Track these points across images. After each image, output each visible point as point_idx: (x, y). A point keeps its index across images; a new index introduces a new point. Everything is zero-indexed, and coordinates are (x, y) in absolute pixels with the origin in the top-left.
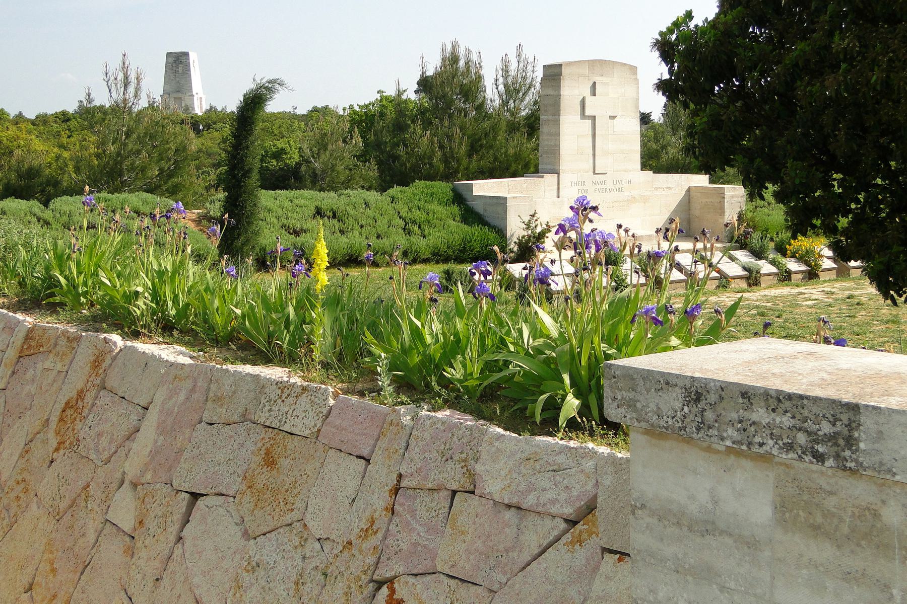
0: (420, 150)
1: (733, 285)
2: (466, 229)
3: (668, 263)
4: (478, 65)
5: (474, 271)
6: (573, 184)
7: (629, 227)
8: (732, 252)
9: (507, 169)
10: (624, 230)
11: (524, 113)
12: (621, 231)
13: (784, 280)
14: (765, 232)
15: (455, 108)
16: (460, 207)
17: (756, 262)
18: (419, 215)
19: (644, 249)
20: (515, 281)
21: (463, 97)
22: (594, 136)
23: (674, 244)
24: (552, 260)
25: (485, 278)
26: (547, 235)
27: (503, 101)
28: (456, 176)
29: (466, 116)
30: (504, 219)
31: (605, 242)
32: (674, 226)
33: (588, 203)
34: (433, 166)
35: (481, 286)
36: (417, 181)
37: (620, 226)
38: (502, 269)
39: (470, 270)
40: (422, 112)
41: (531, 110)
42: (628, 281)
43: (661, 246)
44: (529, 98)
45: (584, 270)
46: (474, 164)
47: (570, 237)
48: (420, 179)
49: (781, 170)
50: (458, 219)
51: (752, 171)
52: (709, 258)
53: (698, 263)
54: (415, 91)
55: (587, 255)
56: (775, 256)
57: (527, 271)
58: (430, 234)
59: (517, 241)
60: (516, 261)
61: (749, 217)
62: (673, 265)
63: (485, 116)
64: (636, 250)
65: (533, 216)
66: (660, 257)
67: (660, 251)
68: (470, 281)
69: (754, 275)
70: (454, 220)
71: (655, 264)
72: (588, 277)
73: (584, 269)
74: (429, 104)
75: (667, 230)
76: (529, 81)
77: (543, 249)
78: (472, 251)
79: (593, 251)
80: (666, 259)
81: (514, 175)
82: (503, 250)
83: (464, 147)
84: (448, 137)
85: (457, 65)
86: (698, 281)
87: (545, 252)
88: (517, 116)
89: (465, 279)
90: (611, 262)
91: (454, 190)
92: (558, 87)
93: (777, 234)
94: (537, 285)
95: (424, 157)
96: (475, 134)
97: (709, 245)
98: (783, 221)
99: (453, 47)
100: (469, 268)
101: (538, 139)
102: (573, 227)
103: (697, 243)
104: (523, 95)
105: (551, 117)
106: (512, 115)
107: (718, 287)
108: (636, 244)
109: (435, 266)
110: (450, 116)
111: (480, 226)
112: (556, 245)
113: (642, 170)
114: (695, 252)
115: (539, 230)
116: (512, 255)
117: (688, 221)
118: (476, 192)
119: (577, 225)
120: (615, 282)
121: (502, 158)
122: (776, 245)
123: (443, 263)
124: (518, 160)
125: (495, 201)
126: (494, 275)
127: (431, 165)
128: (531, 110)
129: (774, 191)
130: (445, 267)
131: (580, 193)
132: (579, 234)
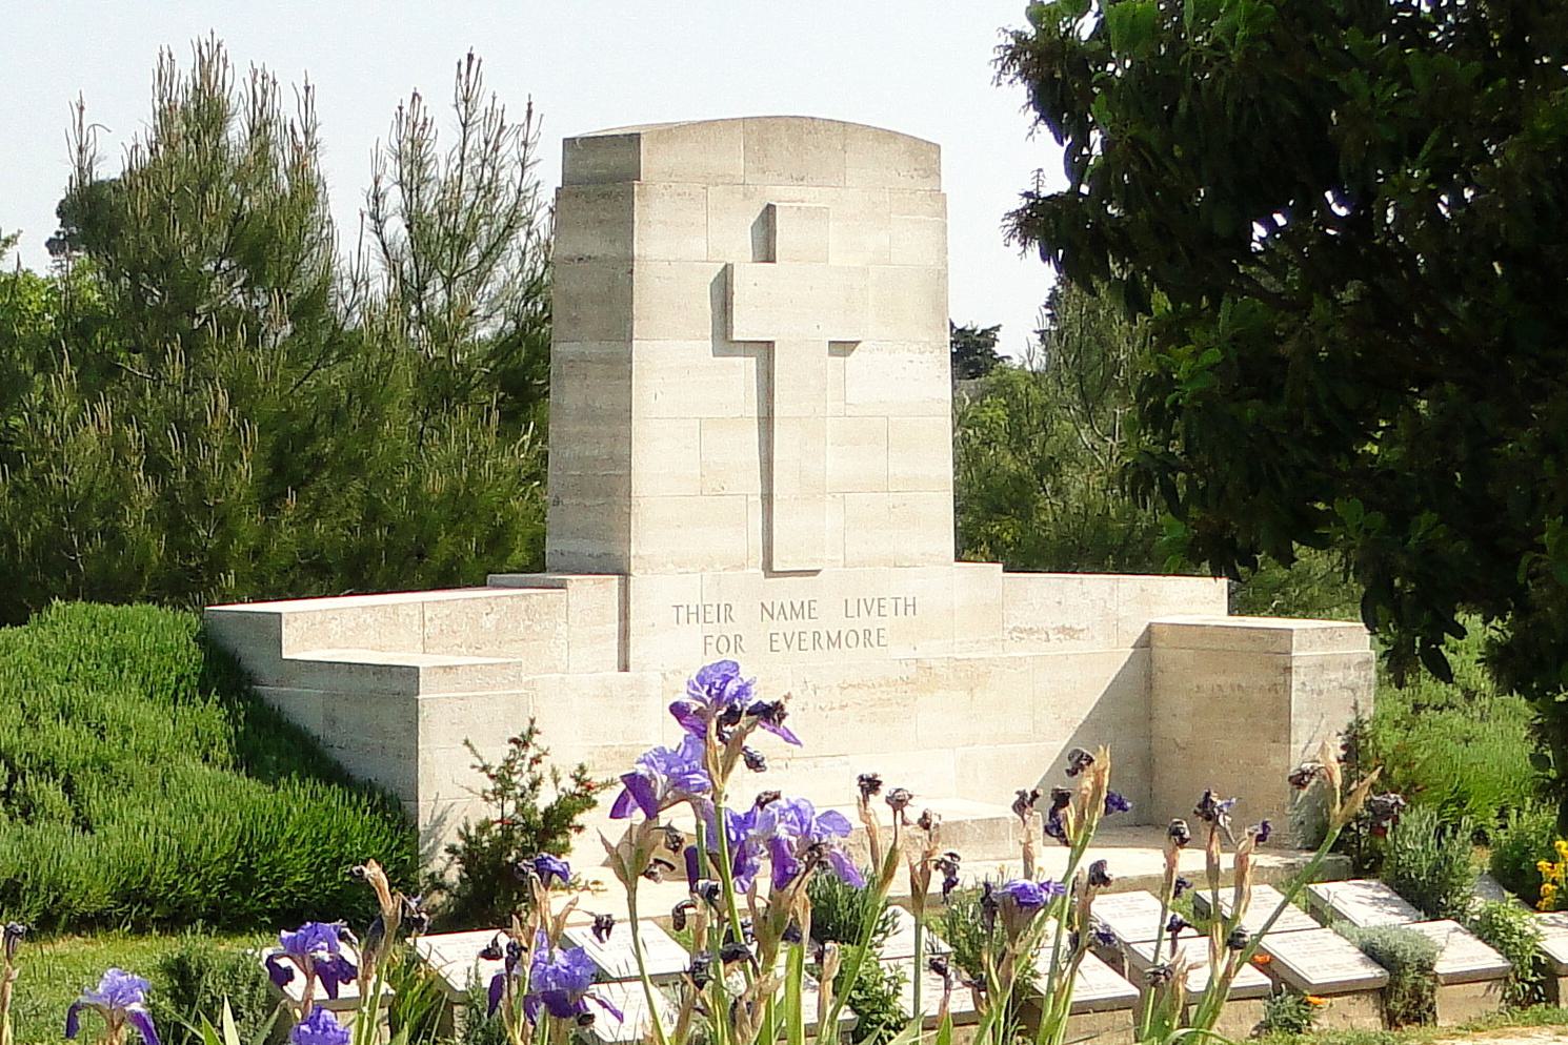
0: (73, 479)
1: (1323, 1022)
2: (254, 796)
3: (1066, 934)
4: (301, 138)
5: (284, 963)
6: (901, 609)
7: (909, 787)
8: (1321, 889)
9: (421, 556)
10: (888, 800)
11: (485, 332)
12: (877, 802)
13: (1530, 1001)
14: (1452, 808)
15: (209, 311)
16: (230, 707)
17: (1418, 927)
18: (65, 740)
19: (970, 875)
20: (450, 1005)
21: (241, 265)
22: (767, 421)
23: (1090, 857)
24: (598, 921)
25: (333, 992)
26: (578, 819)
27: (403, 281)
28: (213, 582)
29: (253, 341)
30: (409, 755)
31: (813, 847)
32: (1087, 782)
33: (742, 691)
34: (122, 544)
35: (313, 1022)
36: (56, 602)
37: (870, 785)
38: (397, 954)
39: (270, 962)
40: (79, 325)
41: (516, 317)
42: (905, 1002)
43: (1037, 862)
44: (507, 272)
45: (727, 960)
46: (287, 535)
47: (669, 828)
48: (70, 596)
49: (1519, 555)
50: (221, 753)
51: (1403, 562)
52: (1228, 912)
53: (1185, 931)
54: (50, 243)
55: (740, 901)
56: (1494, 904)
57: (500, 964)
58: (109, 817)
59: (460, 844)
60: (454, 921)
61: (1387, 748)
62: (1084, 940)
63: (331, 344)
64: (937, 880)
65: (522, 743)
66: (1034, 907)
67: (1032, 884)
68: (272, 1003)
69: (1408, 981)
70: (206, 759)
71: (1013, 936)
72: (742, 987)
73: (729, 958)
74: (105, 296)
75: (1061, 799)
76: (505, 201)
77: (564, 875)
78: (277, 883)
79: (764, 883)
80: (1058, 916)
81: (446, 580)
82: (403, 877)
83: (244, 467)
84: (182, 425)
85: (217, 138)
86: (1186, 1006)
87: (568, 887)
88: (459, 343)
89: (251, 998)
90: (837, 930)
91: (206, 639)
92: (623, 227)
93: (1503, 814)
94: (538, 1019)
95: (84, 505)
96: (293, 416)
97: (1227, 861)
98: (1525, 765)
99: (204, 66)
100: (267, 952)
101: (542, 433)
102: (682, 789)
103: (1180, 851)
104: (484, 256)
105: (593, 348)
106: (441, 336)
107: (1265, 1027)
108: (938, 856)
109: (131, 944)
110: (193, 341)
111: (309, 782)
112: (615, 860)
113: (958, 559)
114: (1174, 886)
115: (546, 798)
116: (438, 898)
117: (1146, 763)
118: (296, 647)
119: (698, 779)
120: (854, 1009)
121: (400, 510)
122: (1498, 861)
123: (163, 931)
124: (461, 518)
125: (370, 682)
126: (366, 978)
127: (114, 537)
128: (516, 317)
129: (1490, 642)
130: (171, 947)
131: (712, 649)
132: (709, 815)
